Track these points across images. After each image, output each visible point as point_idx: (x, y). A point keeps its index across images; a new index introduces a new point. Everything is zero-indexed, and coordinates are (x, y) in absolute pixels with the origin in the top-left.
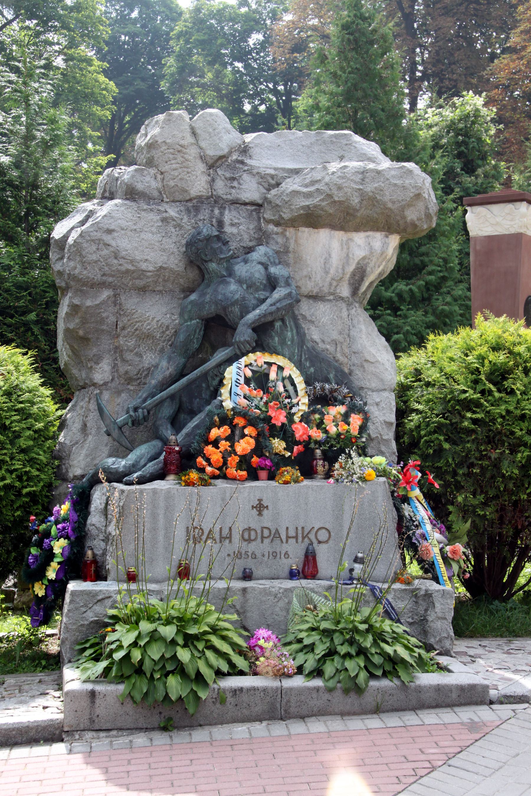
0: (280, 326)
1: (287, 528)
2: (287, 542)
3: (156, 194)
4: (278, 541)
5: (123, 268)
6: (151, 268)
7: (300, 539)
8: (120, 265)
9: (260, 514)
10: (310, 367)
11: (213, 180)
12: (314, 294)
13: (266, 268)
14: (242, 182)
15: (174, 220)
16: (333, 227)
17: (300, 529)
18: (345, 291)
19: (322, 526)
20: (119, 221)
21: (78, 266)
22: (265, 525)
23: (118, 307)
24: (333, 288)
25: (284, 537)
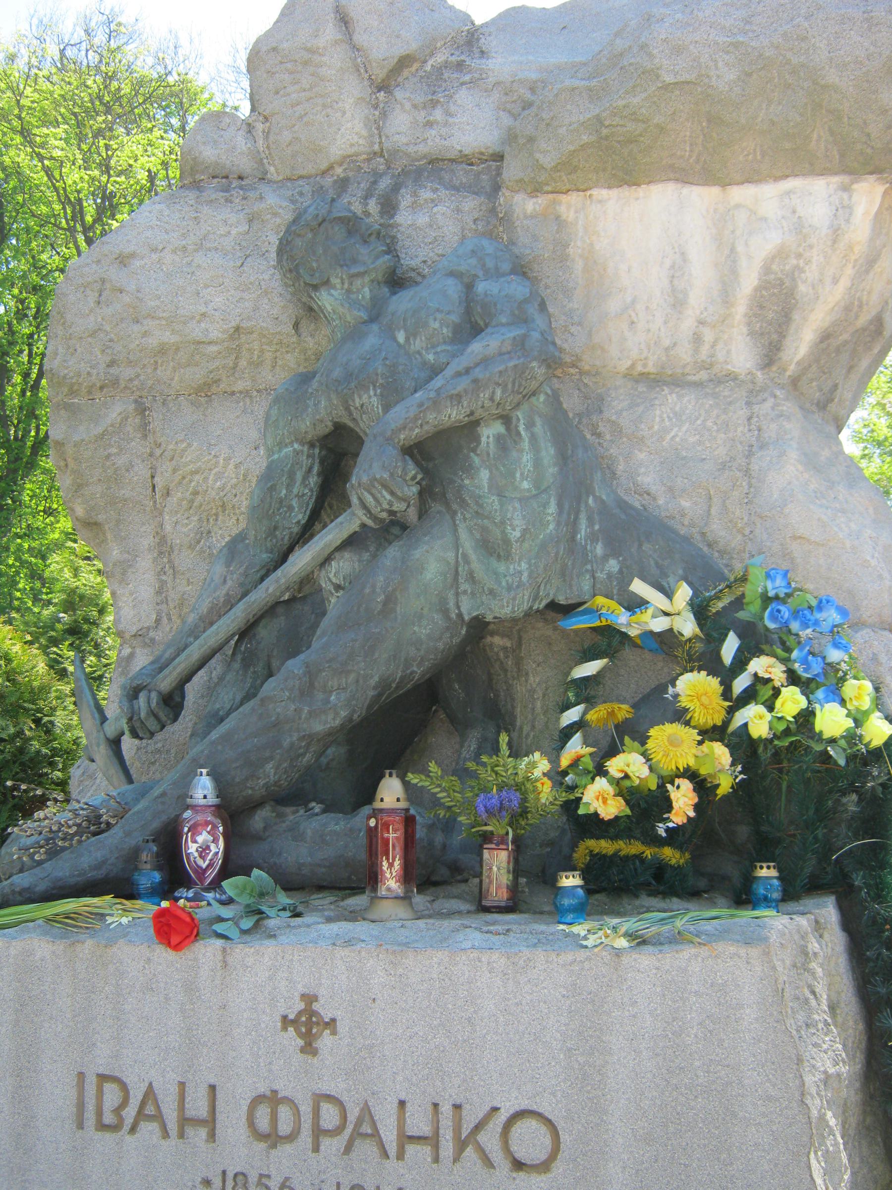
0: (499, 438)
1: (402, 1103)
2: (400, 1156)
3: (245, 164)
4: (366, 1149)
5: (153, 342)
6: (215, 334)
7: (447, 1148)
8: (145, 334)
9: (309, 1048)
10: (605, 558)
11: (384, 115)
12: (651, 368)
13: (469, 287)
14: (453, 108)
15: (275, 215)
16: (683, 175)
17: (446, 1109)
18: (741, 356)
19: (525, 1104)
20: (149, 233)
21: (61, 350)
22: (326, 1087)
23: (150, 438)
24: (705, 350)
25: (390, 1136)
